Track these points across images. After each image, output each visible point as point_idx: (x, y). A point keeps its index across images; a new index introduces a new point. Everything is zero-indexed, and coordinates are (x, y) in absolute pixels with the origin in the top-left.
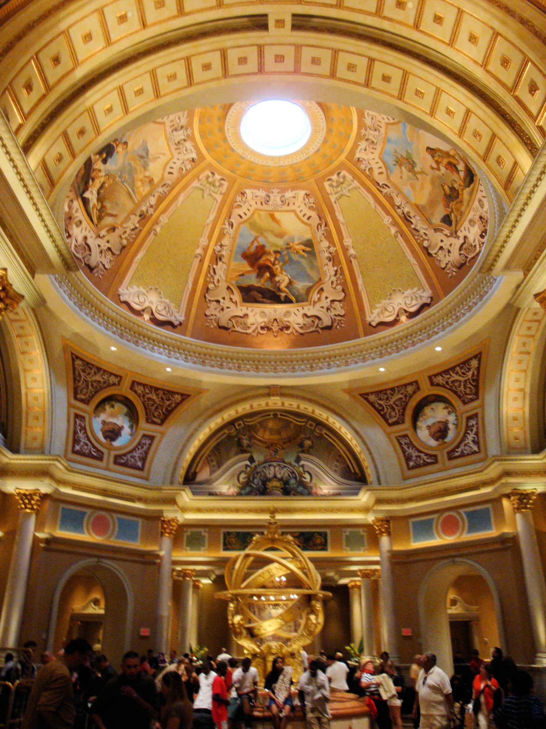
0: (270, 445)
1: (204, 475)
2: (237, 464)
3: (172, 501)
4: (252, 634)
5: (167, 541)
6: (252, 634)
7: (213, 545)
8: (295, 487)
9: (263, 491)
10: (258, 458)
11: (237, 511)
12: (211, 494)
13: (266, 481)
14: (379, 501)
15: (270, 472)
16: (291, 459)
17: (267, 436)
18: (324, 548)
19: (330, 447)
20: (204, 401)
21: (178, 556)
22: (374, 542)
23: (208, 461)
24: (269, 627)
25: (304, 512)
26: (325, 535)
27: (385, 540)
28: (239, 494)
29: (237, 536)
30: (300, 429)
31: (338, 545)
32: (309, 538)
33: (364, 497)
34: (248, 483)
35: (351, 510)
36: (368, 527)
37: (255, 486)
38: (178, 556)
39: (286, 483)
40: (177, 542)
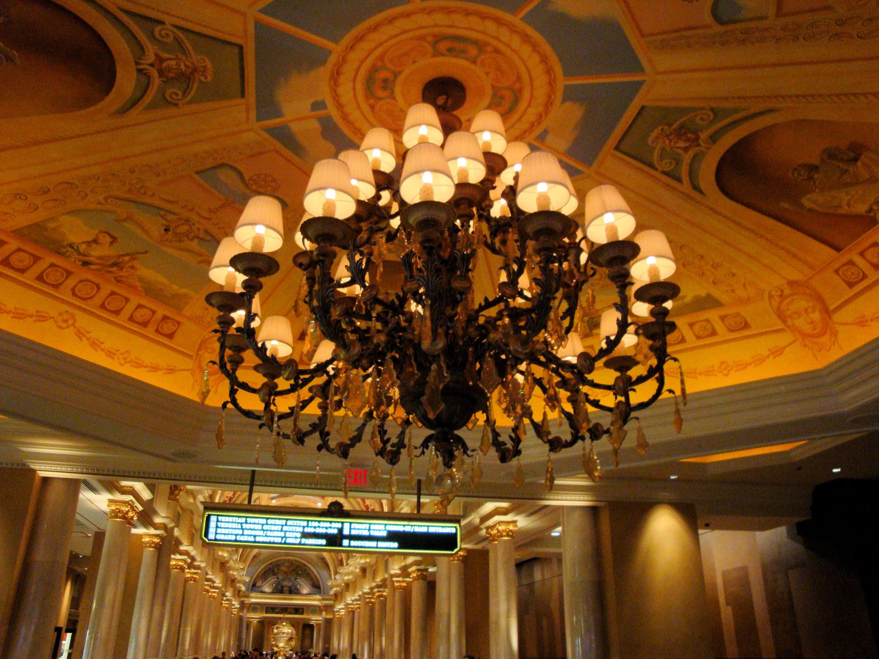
0: (285, 573)
1: (258, 584)
2: (272, 580)
3: (248, 597)
4: (277, 646)
5: (245, 610)
6: (277, 646)
7: (261, 612)
8: (294, 591)
9: (281, 592)
10: (280, 577)
11: (271, 598)
12: (262, 592)
13: (283, 587)
14: (323, 599)
15: (285, 583)
16: (293, 579)
17: (285, 569)
18: (302, 613)
19: (308, 574)
20: (261, 557)
21: (249, 615)
22: (320, 613)
23: (261, 578)
24: (281, 645)
25: (297, 601)
26: (303, 609)
27: (324, 613)
28: (272, 593)
29: (271, 608)
30: (298, 567)
31: (308, 613)
32: (298, 610)
33: (318, 597)
34: (276, 588)
35: (314, 600)
36: (319, 607)
37: (279, 590)
38: (249, 615)
39: (290, 588)
40: (248, 611)
